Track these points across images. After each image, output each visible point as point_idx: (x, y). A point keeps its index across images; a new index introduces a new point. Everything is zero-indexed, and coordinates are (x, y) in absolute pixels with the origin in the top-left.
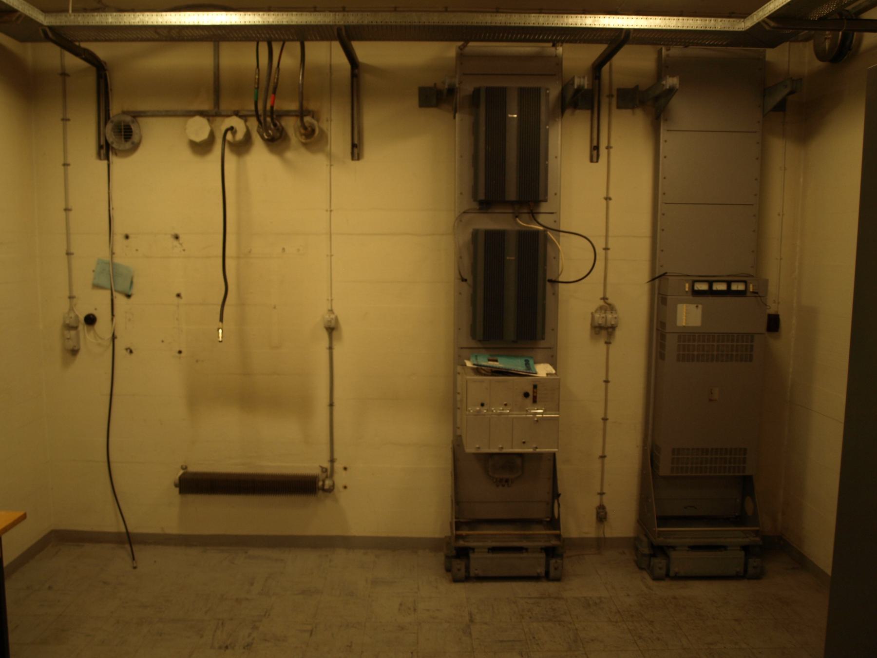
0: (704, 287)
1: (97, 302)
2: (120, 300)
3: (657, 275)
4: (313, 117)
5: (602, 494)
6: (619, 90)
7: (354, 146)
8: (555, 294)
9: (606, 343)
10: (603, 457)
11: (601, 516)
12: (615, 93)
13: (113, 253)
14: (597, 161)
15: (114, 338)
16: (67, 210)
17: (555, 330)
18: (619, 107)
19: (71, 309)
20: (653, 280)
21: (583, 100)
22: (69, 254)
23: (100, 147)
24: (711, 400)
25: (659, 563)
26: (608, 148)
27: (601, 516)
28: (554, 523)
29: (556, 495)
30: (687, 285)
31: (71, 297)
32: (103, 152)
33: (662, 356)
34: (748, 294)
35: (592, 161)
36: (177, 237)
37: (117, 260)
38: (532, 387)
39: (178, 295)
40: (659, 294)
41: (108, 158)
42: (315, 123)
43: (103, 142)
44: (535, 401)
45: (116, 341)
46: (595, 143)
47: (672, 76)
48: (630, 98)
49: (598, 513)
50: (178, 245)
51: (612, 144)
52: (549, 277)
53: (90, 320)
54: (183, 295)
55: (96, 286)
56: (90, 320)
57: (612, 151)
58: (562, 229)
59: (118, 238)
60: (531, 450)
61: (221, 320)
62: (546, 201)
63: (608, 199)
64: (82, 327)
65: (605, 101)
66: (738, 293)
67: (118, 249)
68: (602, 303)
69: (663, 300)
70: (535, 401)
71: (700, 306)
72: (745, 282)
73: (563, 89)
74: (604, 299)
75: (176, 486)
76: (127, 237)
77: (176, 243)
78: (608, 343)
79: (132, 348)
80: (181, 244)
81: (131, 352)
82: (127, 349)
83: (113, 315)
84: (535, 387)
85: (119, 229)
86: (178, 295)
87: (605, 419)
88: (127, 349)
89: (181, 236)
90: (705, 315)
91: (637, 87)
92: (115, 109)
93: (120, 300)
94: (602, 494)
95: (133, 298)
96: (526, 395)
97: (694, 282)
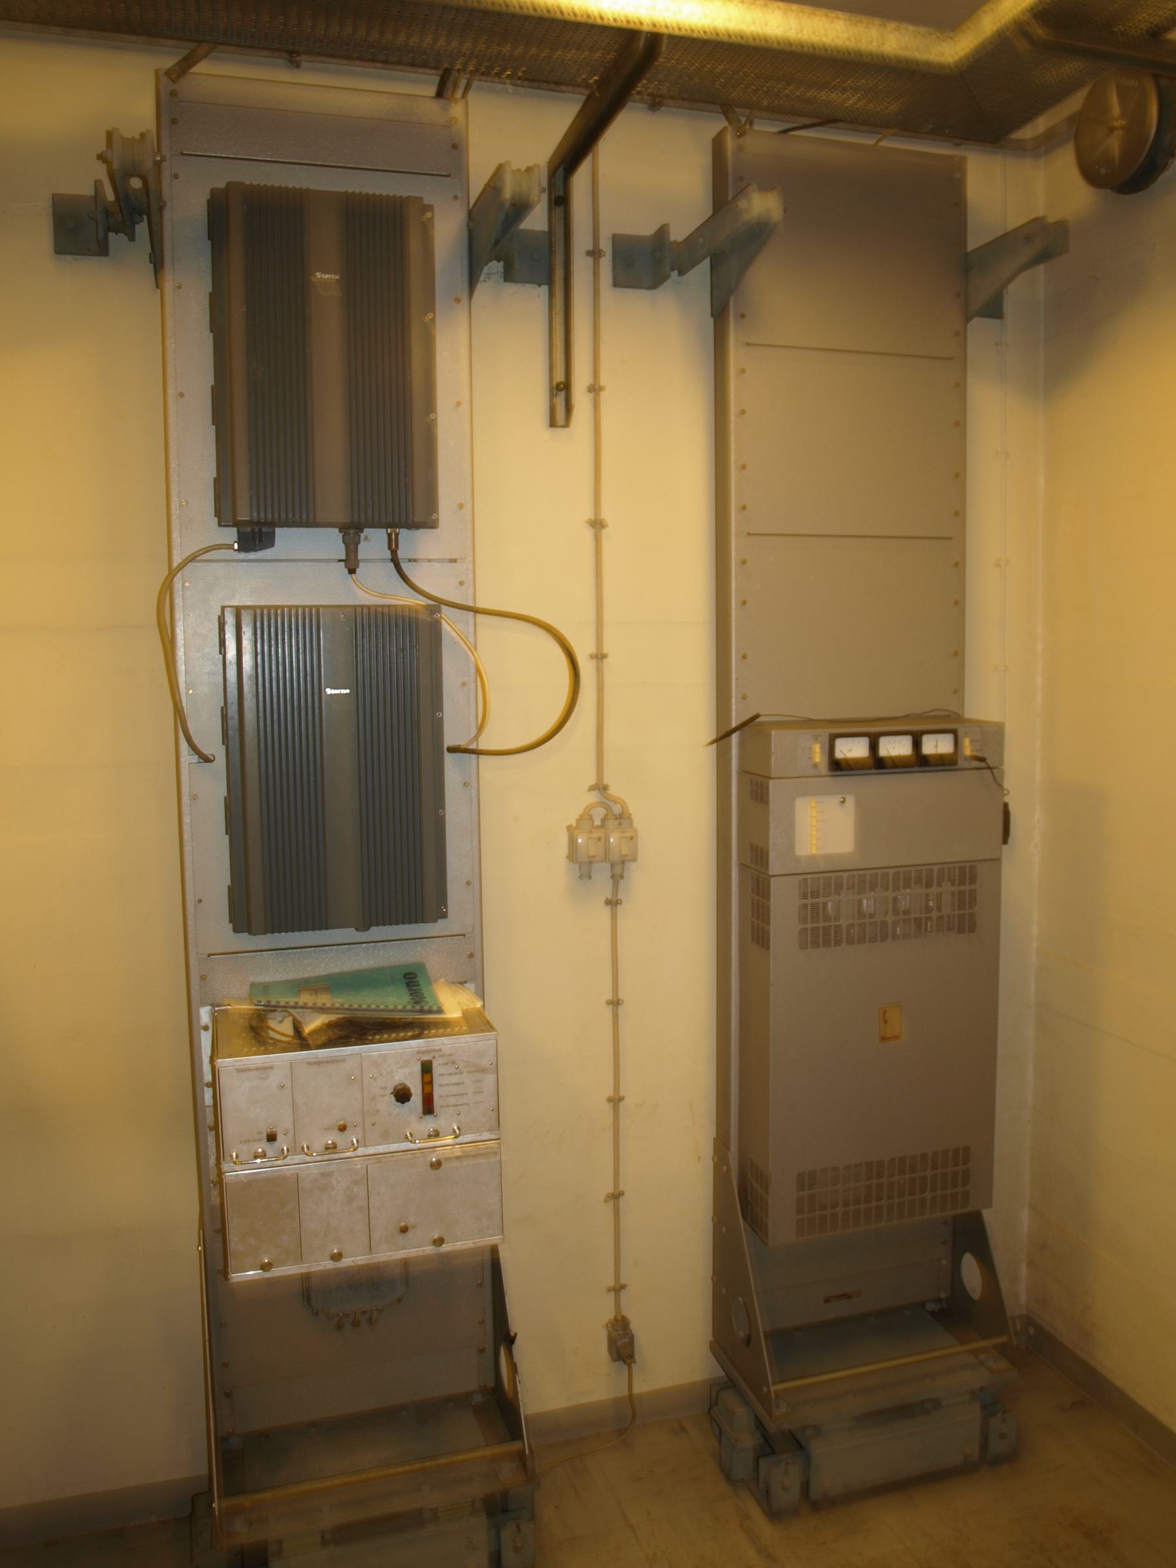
0: (853, 749)
3: (734, 725)
5: (618, 1289)
6: (616, 239)
8: (471, 785)
9: (608, 902)
10: (616, 1197)
11: (622, 1346)
12: (606, 246)
14: (567, 424)
17: (475, 884)
18: (616, 284)
20: (722, 738)
21: (520, 245)
24: (883, 1039)
25: (785, 1478)
26: (595, 389)
27: (622, 1346)
28: (500, 1408)
29: (505, 1338)
30: (817, 748)
33: (758, 934)
34: (961, 763)
35: (553, 424)
38: (417, 1068)
40: (743, 772)
44: (428, 1107)
46: (560, 377)
47: (765, 188)
48: (644, 263)
49: (612, 1342)
51: (604, 380)
52: (449, 740)
57: (604, 395)
58: (480, 604)
60: (429, 1250)
62: (433, 525)
63: (597, 525)
65: (581, 266)
66: (944, 763)
68: (593, 797)
69: (757, 790)
70: (428, 1107)
71: (850, 801)
72: (954, 732)
73: (470, 215)
74: (601, 788)
78: (613, 903)
84: (427, 1069)
87: (616, 1101)
90: (867, 826)
91: (662, 232)
94: (618, 1289)
96: (402, 1095)
97: (833, 738)
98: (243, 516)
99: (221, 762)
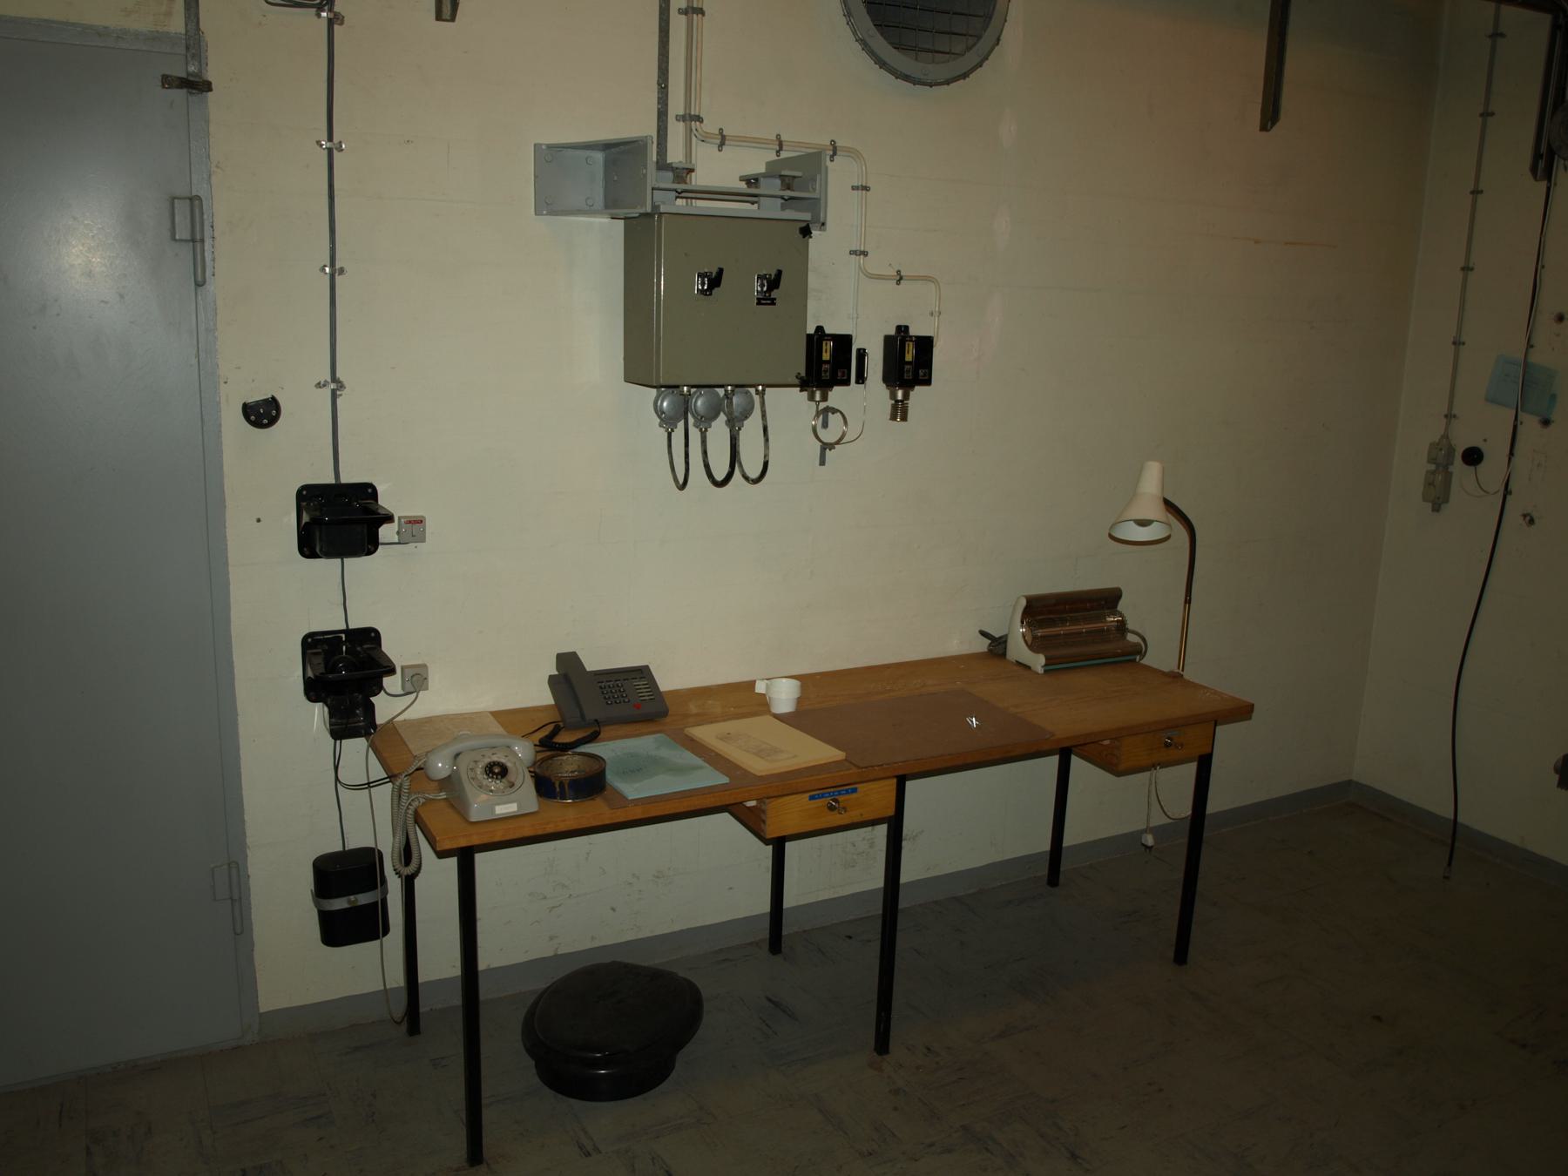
1: (1484, 425)
2: (1530, 423)
13: (1530, 346)
15: (1507, 491)
19: (1445, 436)
23: (1537, 156)
31: (1450, 416)
32: (1541, 164)
37: (1534, 358)
41: (1548, 175)
43: (1543, 149)
53: (1473, 457)
55: (1492, 400)
56: (1473, 457)
75: (1556, 771)
79: (1535, 515)
81: (1532, 521)
82: (1525, 516)
83: (1511, 453)
88: (1525, 516)
93: (1530, 423)
95: (1552, 426)
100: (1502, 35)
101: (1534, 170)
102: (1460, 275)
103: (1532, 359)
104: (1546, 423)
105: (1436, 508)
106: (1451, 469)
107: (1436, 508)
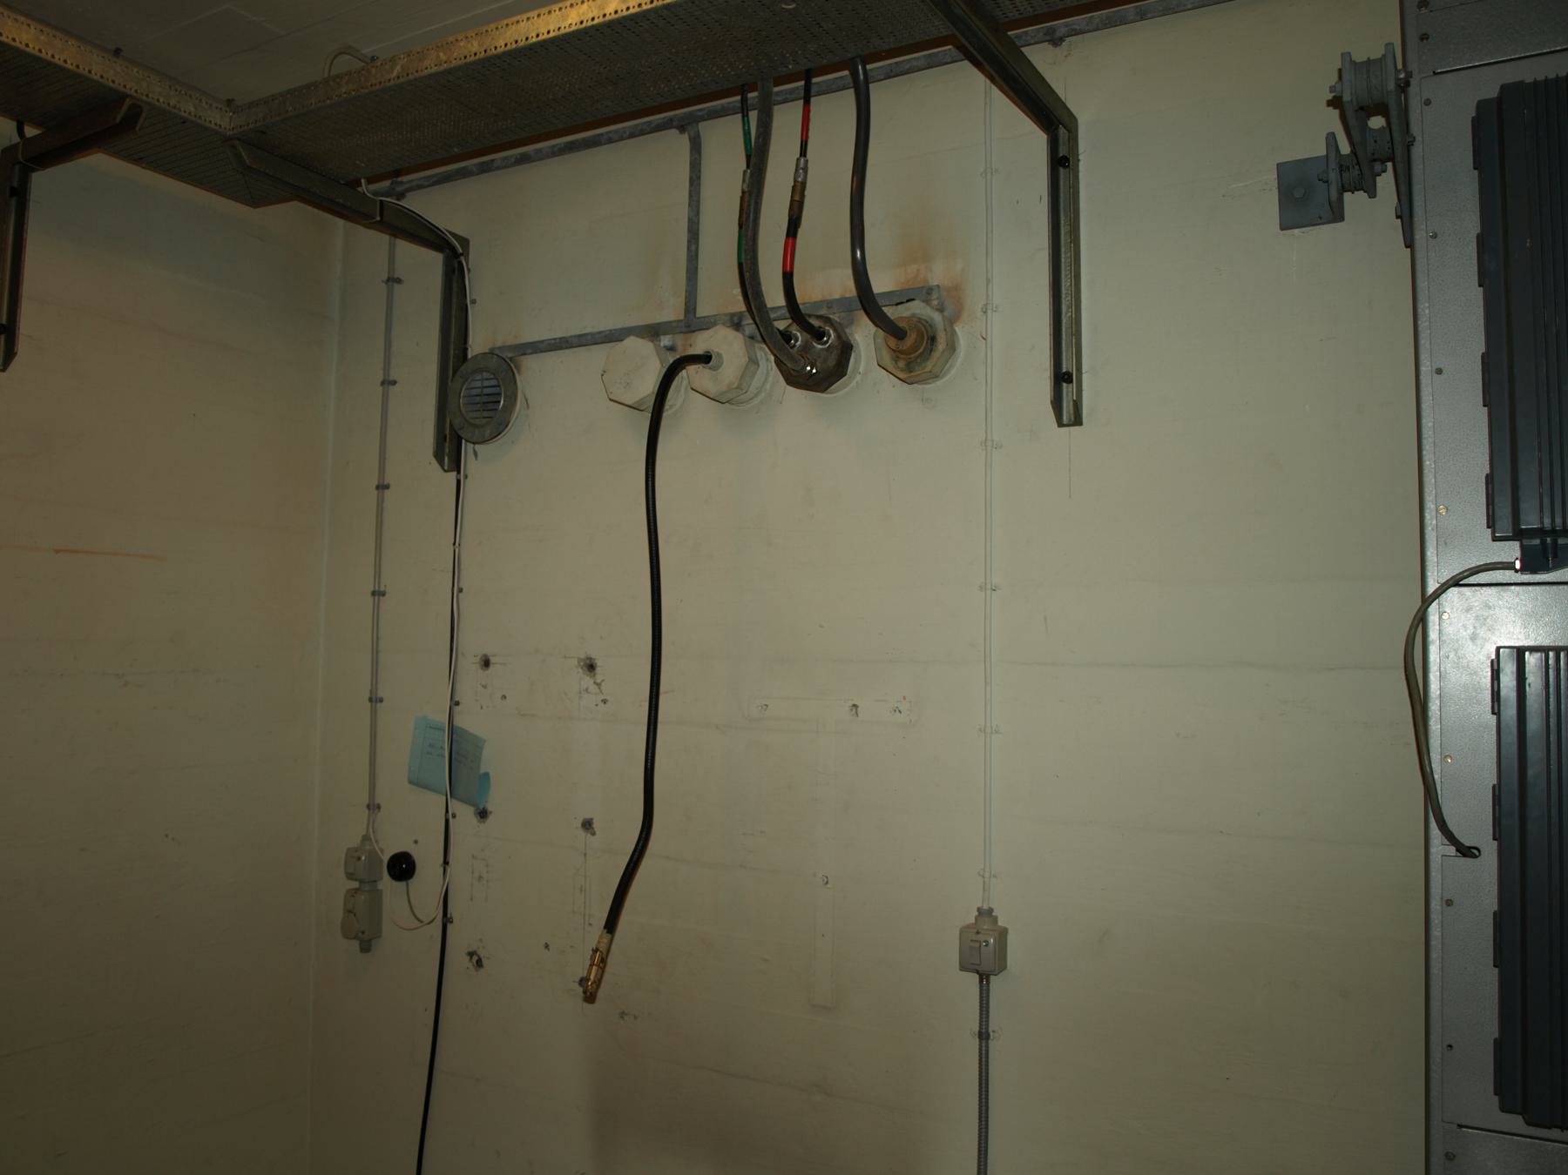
1: (412, 822)
4: (927, 302)
7: (1062, 378)
15: (446, 920)
16: (378, 594)
19: (366, 838)
22: (375, 700)
23: (441, 438)
31: (373, 807)
36: (591, 667)
37: (464, 721)
39: (587, 825)
41: (456, 465)
42: (937, 317)
45: (449, 927)
50: (593, 688)
53: (402, 867)
54: (595, 825)
56: (402, 867)
59: (468, 665)
61: (611, 925)
64: (386, 882)
67: (463, 694)
76: (486, 663)
77: (588, 681)
79: (482, 953)
80: (598, 685)
81: (479, 964)
82: (471, 954)
83: (446, 862)
85: (472, 643)
86: (587, 825)
88: (471, 954)
89: (599, 663)
92: (478, 344)
98: (1530, 521)
99: (1490, 850)
100: (399, 281)
101: (439, 455)
102: (370, 599)
103: (459, 722)
104: (483, 814)
105: (366, 947)
106: (380, 886)
107: (366, 947)
